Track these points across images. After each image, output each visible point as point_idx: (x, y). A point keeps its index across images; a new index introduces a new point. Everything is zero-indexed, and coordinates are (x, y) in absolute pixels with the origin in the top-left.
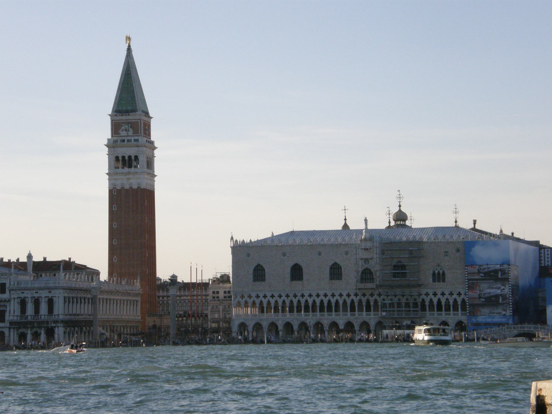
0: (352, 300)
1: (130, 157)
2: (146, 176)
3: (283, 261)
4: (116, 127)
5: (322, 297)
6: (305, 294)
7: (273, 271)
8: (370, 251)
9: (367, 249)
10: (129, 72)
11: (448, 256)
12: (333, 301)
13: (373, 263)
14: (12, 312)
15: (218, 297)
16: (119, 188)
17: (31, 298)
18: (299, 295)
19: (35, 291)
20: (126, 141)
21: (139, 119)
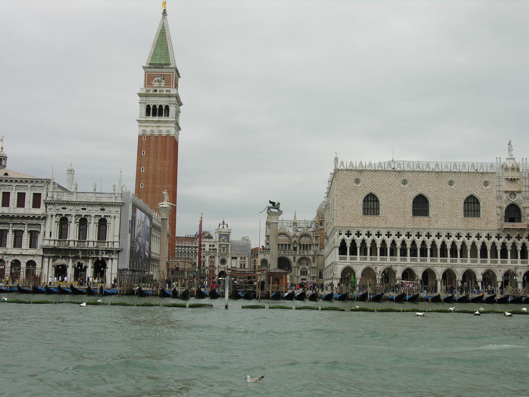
0: (494, 244)
1: (161, 106)
3: (403, 191)
4: (149, 80)
7: (390, 202)
9: (515, 179)
10: (164, 32)
12: (469, 243)
13: (521, 198)
14: (47, 236)
15: (204, 249)
16: (148, 133)
17: (75, 216)
19: (82, 207)
20: (158, 91)
21: (171, 72)
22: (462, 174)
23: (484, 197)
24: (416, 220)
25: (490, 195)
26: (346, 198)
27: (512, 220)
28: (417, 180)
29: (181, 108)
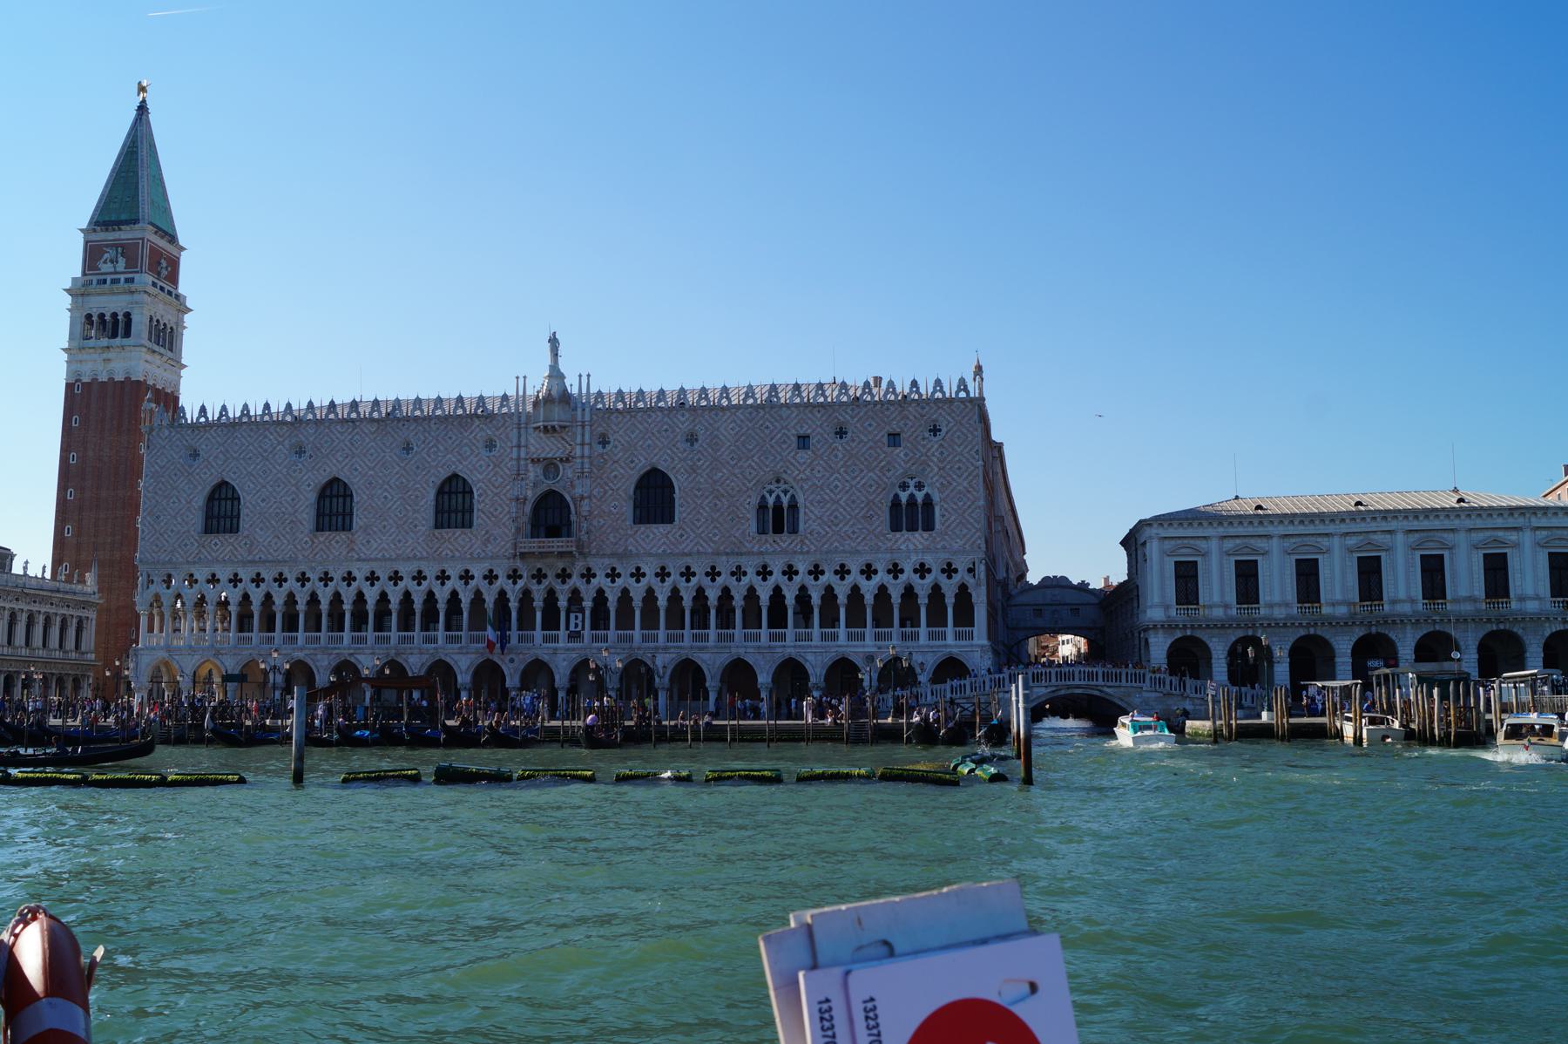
0: (502, 593)
1: (114, 315)
2: (149, 357)
3: (295, 471)
4: (92, 255)
5: (407, 583)
6: (356, 573)
7: (263, 500)
8: (564, 435)
9: (553, 427)
11: (809, 448)
12: (442, 595)
13: (570, 476)
16: (86, 379)
18: (337, 575)
20: (108, 282)
22: (433, 422)
23: (481, 477)
24: (320, 543)
25: (497, 473)
26: (166, 494)
27: (554, 532)
28: (326, 442)
29: (187, 317)
